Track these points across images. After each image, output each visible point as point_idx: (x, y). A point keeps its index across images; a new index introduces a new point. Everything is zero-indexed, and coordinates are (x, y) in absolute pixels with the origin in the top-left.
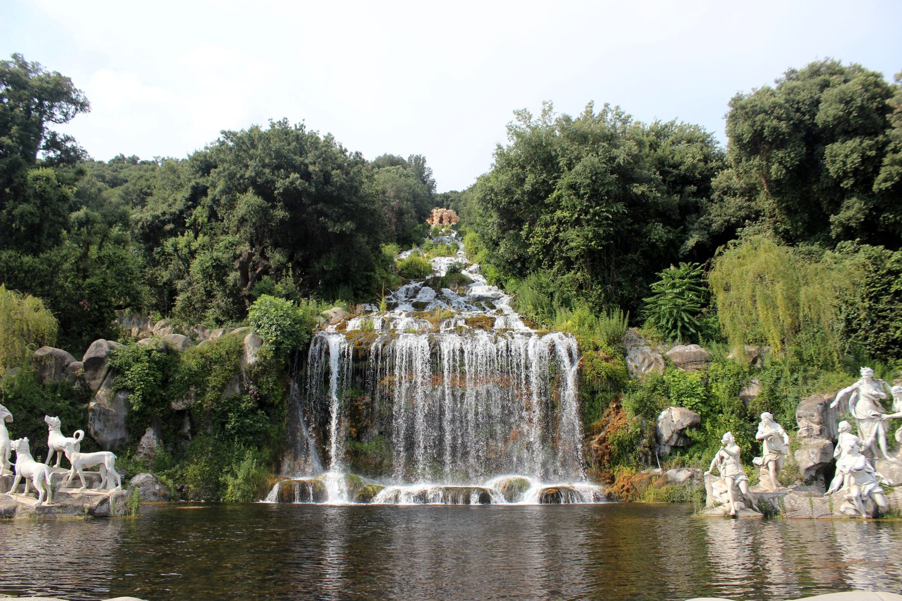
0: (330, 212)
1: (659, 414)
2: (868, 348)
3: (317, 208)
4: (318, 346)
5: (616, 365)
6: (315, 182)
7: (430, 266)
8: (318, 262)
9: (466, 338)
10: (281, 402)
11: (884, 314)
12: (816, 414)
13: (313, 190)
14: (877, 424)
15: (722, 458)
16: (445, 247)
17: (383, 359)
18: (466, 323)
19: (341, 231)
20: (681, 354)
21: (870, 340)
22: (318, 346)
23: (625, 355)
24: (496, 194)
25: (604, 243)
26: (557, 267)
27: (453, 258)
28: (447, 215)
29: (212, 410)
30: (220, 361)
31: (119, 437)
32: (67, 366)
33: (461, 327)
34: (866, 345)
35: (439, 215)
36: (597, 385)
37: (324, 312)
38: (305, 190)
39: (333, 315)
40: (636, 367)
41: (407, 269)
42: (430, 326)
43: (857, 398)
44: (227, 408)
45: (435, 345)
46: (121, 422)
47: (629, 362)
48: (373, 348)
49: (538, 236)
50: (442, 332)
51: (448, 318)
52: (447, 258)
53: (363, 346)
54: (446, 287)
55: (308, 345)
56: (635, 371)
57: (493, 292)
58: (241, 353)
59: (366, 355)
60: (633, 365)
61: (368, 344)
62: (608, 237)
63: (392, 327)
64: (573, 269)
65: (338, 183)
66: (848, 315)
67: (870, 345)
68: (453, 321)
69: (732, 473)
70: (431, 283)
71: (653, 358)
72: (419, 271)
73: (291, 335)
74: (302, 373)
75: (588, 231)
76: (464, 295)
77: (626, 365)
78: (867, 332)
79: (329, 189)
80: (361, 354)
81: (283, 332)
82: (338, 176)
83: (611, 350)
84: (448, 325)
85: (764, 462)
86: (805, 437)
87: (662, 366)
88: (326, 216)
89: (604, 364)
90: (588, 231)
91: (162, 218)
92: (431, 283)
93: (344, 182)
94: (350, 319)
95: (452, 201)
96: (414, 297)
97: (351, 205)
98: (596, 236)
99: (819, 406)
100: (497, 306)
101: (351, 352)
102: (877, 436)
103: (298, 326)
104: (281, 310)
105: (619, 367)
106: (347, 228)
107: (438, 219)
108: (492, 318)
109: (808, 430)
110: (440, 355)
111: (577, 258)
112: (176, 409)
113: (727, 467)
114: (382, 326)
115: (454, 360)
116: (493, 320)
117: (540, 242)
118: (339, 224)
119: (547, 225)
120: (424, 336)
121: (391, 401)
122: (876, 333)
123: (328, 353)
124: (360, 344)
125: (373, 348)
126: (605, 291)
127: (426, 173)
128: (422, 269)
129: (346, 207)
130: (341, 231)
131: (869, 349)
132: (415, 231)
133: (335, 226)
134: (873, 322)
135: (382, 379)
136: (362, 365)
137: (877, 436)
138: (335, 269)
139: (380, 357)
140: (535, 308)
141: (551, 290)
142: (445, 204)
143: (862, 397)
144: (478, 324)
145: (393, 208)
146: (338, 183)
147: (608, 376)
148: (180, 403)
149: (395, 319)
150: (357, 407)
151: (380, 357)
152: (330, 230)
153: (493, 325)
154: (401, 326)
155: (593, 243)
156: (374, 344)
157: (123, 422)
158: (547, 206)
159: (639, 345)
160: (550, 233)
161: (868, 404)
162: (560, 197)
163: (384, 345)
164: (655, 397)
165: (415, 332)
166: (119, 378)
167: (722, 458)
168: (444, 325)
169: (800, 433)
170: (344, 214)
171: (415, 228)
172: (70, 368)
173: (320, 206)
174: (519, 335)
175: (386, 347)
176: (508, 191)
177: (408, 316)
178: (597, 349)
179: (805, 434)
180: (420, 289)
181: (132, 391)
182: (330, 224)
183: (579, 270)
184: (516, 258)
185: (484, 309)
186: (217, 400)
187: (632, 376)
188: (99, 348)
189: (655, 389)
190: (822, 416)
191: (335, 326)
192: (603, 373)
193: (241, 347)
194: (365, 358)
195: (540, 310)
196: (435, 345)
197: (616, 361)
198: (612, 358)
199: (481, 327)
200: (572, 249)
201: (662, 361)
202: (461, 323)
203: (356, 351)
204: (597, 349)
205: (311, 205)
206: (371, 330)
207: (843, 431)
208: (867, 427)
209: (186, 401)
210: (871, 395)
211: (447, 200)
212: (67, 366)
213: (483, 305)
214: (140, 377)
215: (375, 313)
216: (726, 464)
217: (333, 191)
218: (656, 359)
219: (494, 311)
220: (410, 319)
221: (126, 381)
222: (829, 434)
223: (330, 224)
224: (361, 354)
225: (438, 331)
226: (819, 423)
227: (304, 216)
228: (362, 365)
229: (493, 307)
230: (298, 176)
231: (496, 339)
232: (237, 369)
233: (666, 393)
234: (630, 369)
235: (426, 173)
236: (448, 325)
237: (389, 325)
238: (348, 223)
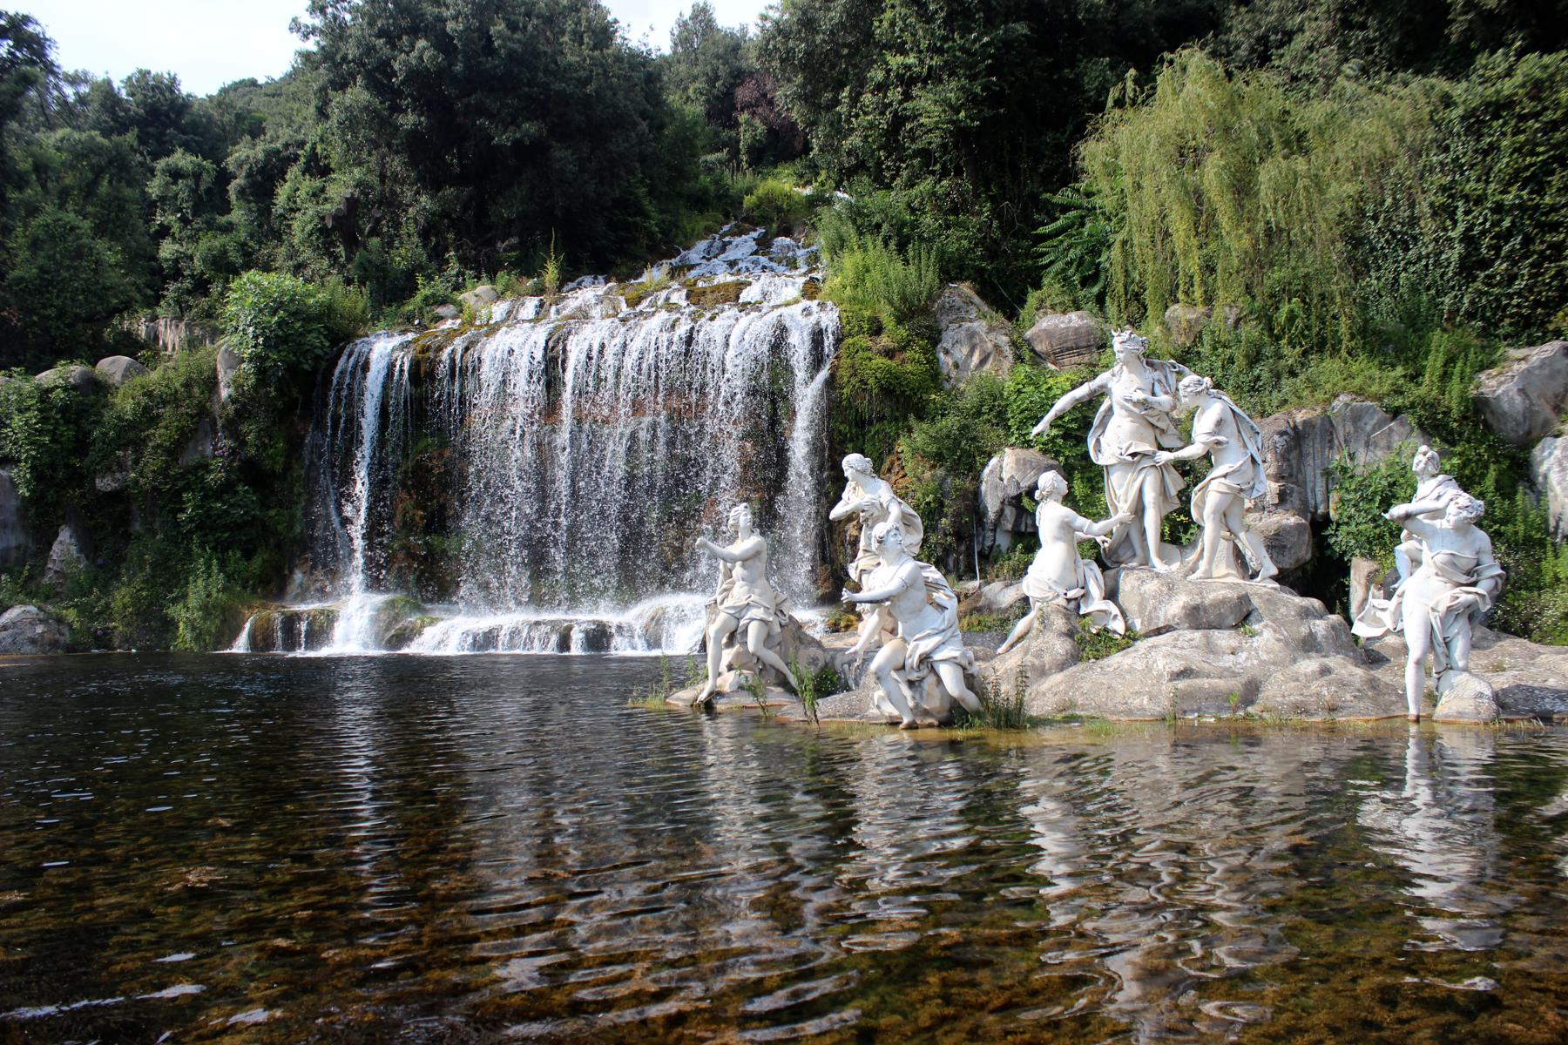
1: (984, 465)
2: (1515, 302)
4: (352, 360)
5: (910, 364)
11: (1554, 217)
20: (1049, 334)
21: (1519, 284)
23: (934, 337)
25: (987, 113)
29: (154, 488)
30: (172, 399)
31: (13, 543)
34: (1510, 297)
36: (863, 405)
40: (956, 366)
44: (180, 484)
46: (13, 518)
47: (942, 356)
48: (445, 355)
53: (431, 354)
56: (953, 374)
58: (212, 383)
60: (950, 361)
61: (440, 349)
62: (994, 98)
64: (933, 173)
66: (1470, 229)
67: (1519, 294)
71: (990, 346)
75: (951, 89)
77: (933, 362)
78: (1514, 263)
79: (489, 63)
83: (903, 332)
89: (880, 361)
90: (951, 89)
91: (285, 154)
98: (972, 100)
101: (406, 367)
102: (1139, 510)
105: (909, 367)
106: (526, 134)
122: (1532, 265)
126: (997, 213)
131: (1518, 306)
134: (1528, 240)
137: (1139, 510)
147: (881, 387)
155: (962, 114)
156: (449, 349)
157: (14, 518)
159: (963, 320)
163: (467, 349)
164: (981, 427)
178: (877, 330)
186: (163, 472)
187: (947, 386)
189: (979, 413)
192: (871, 381)
194: (431, 376)
197: (908, 354)
198: (903, 349)
201: (1008, 351)
203: (415, 365)
204: (877, 330)
209: (118, 476)
217: (496, 67)
218: (996, 346)
222: (1305, 502)
226: (1279, 477)
232: (203, 412)
233: (1001, 418)
234: (945, 371)
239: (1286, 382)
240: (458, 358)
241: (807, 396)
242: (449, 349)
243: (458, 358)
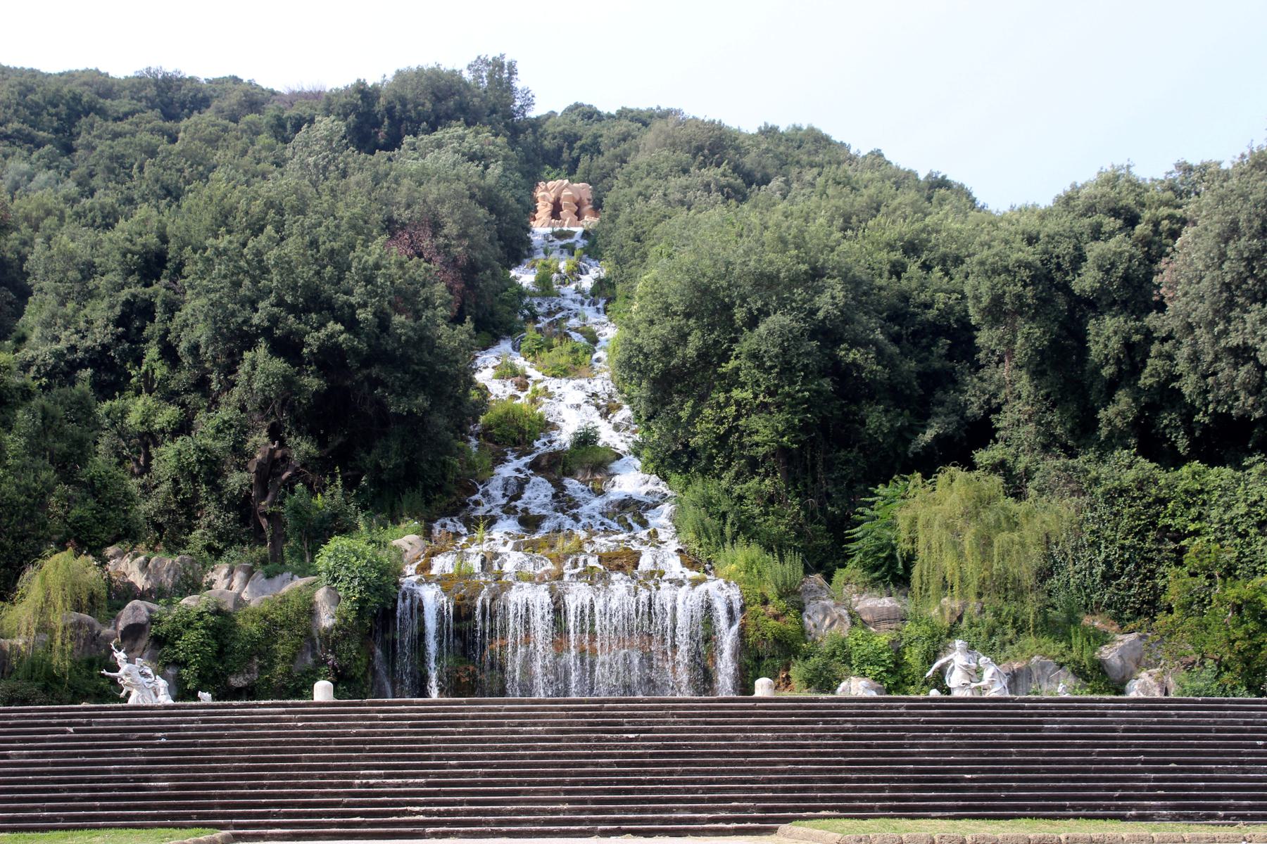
0: (390, 380)
1: (837, 686)
3: (370, 374)
4: (408, 601)
5: (789, 625)
6: (367, 335)
7: (541, 417)
8: (369, 453)
9: (598, 589)
10: (365, 675)
13: (363, 346)
16: (568, 347)
17: (493, 616)
18: (600, 561)
19: (410, 412)
20: (871, 610)
22: (408, 601)
23: (801, 609)
24: (646, 356)
25: (803, 437)
26: (736, 469)
27: (583, 382)
28: (572, 198)
29: (284, 687)
30: (288, 624)
32: (98, 635)
33: (592, 568)
35: (551, 196)
36: (762, 648)
37: (395, 542)
38: (354, 350)
39: (408, 547)
40: (815, 626)
41: (498, 425)
42: (549, 566)
44: (301, 683)
45: (558, 598)
47: (806, 619)
48: (479, 604)
49: (707, 422)
50: (566, 578)
51: (575, 552)
52: (572, 382)
53: (466, 601)
54: (571, 474)
55: (395, 601)
56: (813, 631)
57: (650, 487)
58: (310, 611)
59: (470, 613)
60: (811, 623)
61: (472, 598)
62: (806, 427)
63: (496, 568)
64: (759, 474)
65: (403, 338)
68: (582, 558)
70: (544, 462)
71: (836, 615)
72: (521, 431)
73: (377, 590)
74: (388, 636)
75: (779, 419)
76: (600, 493)
77: (802, 623)
80: (464, 611)
81: (368, 587)
82: (403, 325)
83: (783, 604)
84: (575, 565)
87: (847, 625)
88: (384, 385)
89: (772, 622)
90: (779, 419)
91: (70, 357)
92: (544, 462)
93: (411, 334)
94: (433, 554)
95: (583, 149)
96: (517, 497)
97: (424, 368)
98: (790, 427)
100: (651, 521)
101: (451, 610)
103: (385, 578)
104: (364, 558)
105: (790, 627)
106: (418, 407)
107: (550, 207)
108: (635, 553)
110: (565, 612)
111: (765, 456)
112: (237, 686)
114: (482, 568)
115: (582, 619)
116: (638, 555)
117: (711, 430)
118: (405, 399)
119: (720, 407)
120: (545, 586)
121: (502, 669)
123: (421, 609)
124: (462, 598)
125: (479, 604)
126: (804, 506)
127: (518, 103)
128: (527, 428)
129: (414, 370)
130: (410, 412)
132: (503, 301)
133: (399, 402)
135: (491, 643)
136: (465, 625)
138: (397, 466)
139: (488, 617)
140: (699, 536)
141: (723, 508)
142: (565, 155)
144: (616, 562)
145: (455, 260)
146: (403, 338)
147: (775, 638)
148: (241, 678)
149: (500, 554)
150: (459, 679)
151: (488, 617)
152: (393, 409)
153: (636, 566)
154: (509, 567)
155: (785, 439)
156: (480, 598)
158: (723, 376)
159: (819, 598)
160: (725, 417)
162: (737, 370)
163: (493, 600)
164: (835, 664)
165: (530, 579)
166: (167, 649)
168: (568, 564)
170: (412, 381)
171: (504, 295)
172: (102, 638)
173: (375, 371)
174: (667, 584)
175: (497, 602)
176: (666, 351)
177: (516, 548)
178: (765, 602)
180: (527, 481)
181: (184, 664)
182: (391, 399)
183: (767, 475)
184: (680, 447)
185: (630, 528)
186: (288, 673)
187: (810, 638)
188: (137, 612)
189: (834, 655)
191: (414, 566)
193: (312, 605)
194: (470, 616)
195: (705, 540)
196: (558, 598)
197: (788, 618)
198: (783, 615)
199: (620, 568)
200: (757, 444)
201: (847, 618)
202: (593, 562)
203: (457, 608)
204: (765, 602)
205: (359, 369)
206: (471, 575)
209: (247, 676)
211: (571, 148)
212: (98, 635)
213: (630, 521)
214: (195, 647)
215: (464, 539)
217: (394, 350)
218: (840, 616)
219: (643, 534)
220: (520, 554)
221: (176, 653)
223: (391, 399)
224: (464, 611)
225: (560, 577)
227: (348, 383)
228: (465, 625)
229: (644, 524)
230: (342, 328)
231: (636, 589)
232: (308, 635)
233: (847, 660)
234: (808, 629)
235: (518, 103)
236: (575, 565)
237: (491, 564)
238: (420, 400)
239: (1008, 647)
240: (488, 604)
241: (728, 639)
242: (480, 598)
243: (488, 604)
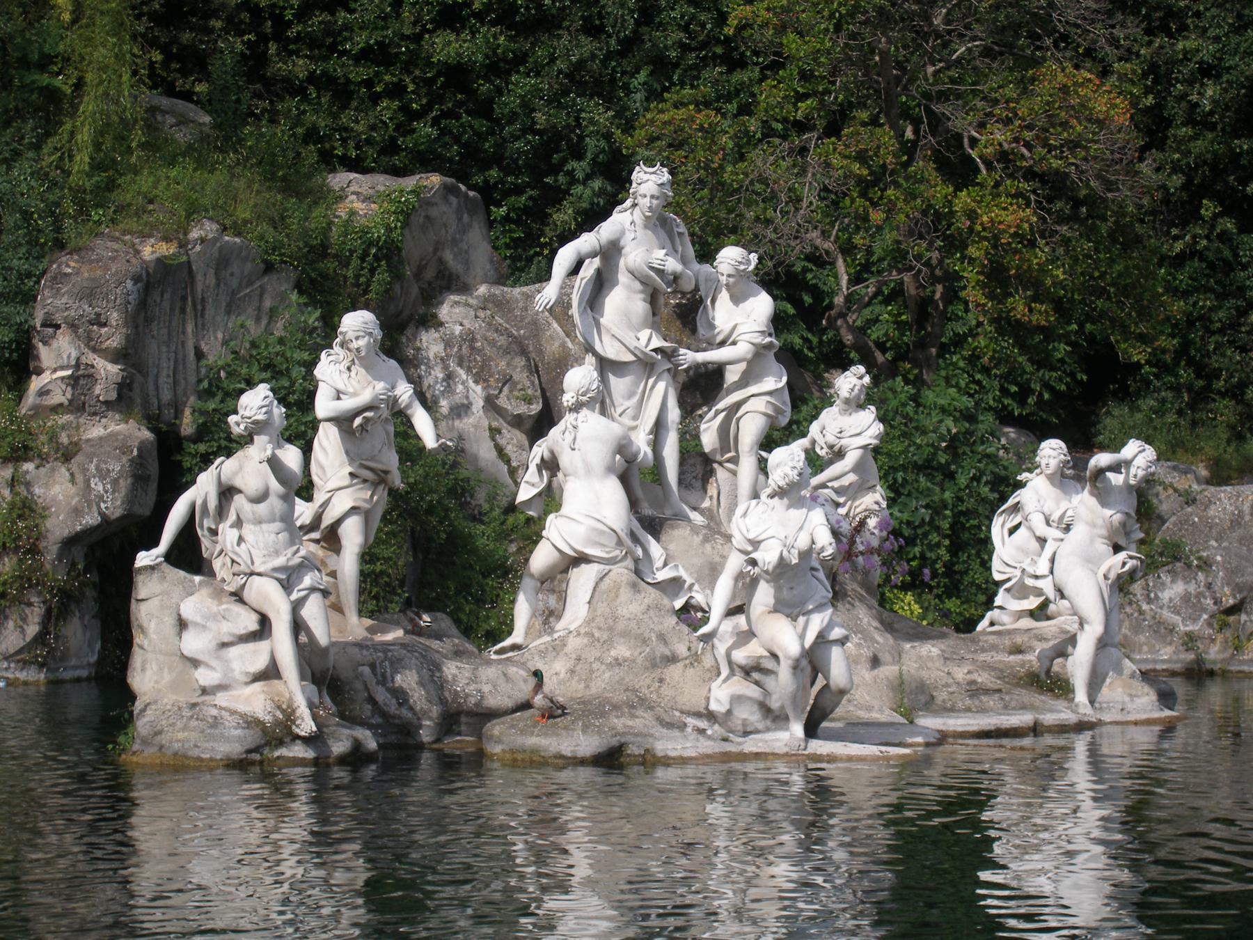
12: (114, 317)
14: (661, 385)
15: (227, 492)
43: (601, 283)
69: (280, 561)
85: (318, 518)
86: (56, 409)
99: (129, 284)
109: (74, 381)
113: (248, 531)
143: (623, 277)
161: (640, 306)
167: (227, 492)
169: (43, 392)
179: (59, 396)
190: (136, 327)
207: (577, 408)
208: (630, 396)
210: (660, 272)
216: (239, 523)
222: (146, 404)
226: (117, 356)
